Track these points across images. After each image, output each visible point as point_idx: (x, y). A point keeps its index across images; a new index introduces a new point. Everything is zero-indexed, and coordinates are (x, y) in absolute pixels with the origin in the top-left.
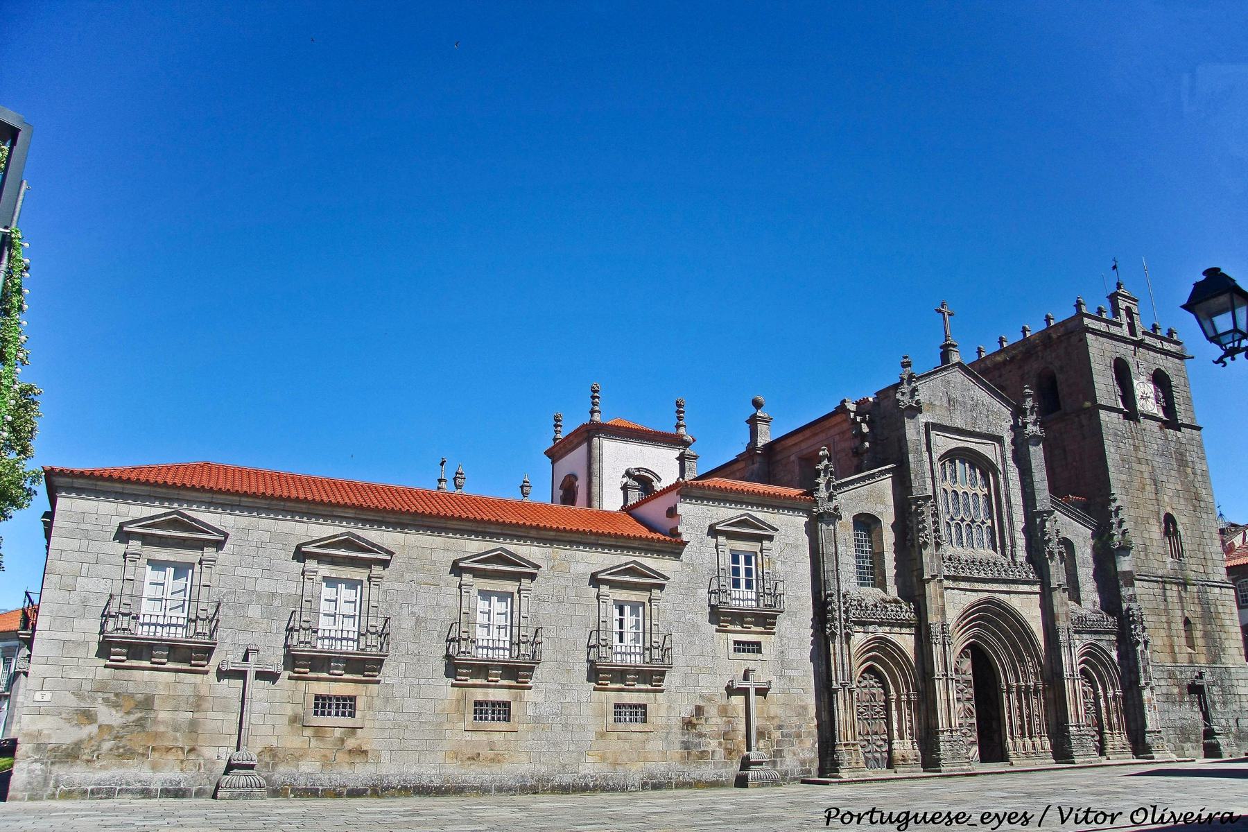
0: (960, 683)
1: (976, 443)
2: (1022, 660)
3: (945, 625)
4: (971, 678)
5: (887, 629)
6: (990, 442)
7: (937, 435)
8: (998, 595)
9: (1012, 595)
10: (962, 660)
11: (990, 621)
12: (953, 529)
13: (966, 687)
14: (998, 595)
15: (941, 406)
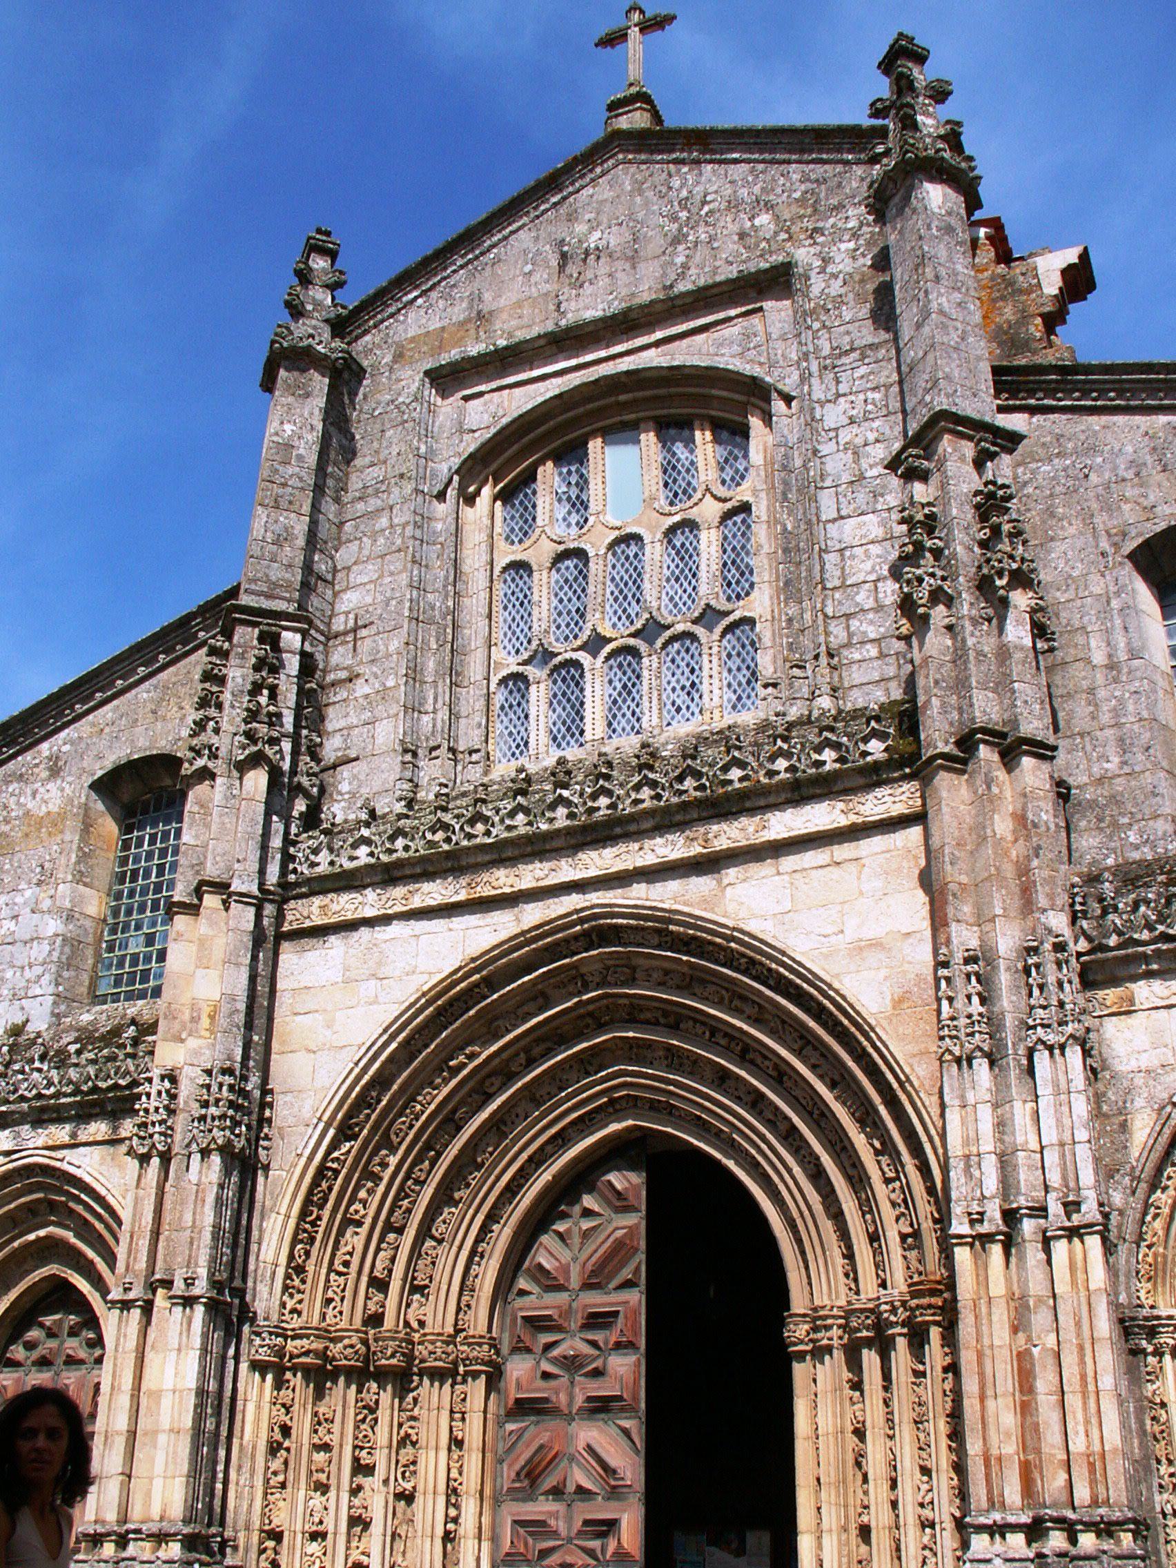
0: (559, 1329)
1: (657, 344)
2: (858, 1180)
3: (209, 1072)
4: (636, 1298)
5: (61, 1133)
6: (733, 313)
7: (466, 399)
8: (640, 895)
9: (732, 873)
10: (586, 1224)
11: (675, 1019)
12: (539, 695)
13: (594, 1344)
14: (640, 895)
15: (519, 304)
